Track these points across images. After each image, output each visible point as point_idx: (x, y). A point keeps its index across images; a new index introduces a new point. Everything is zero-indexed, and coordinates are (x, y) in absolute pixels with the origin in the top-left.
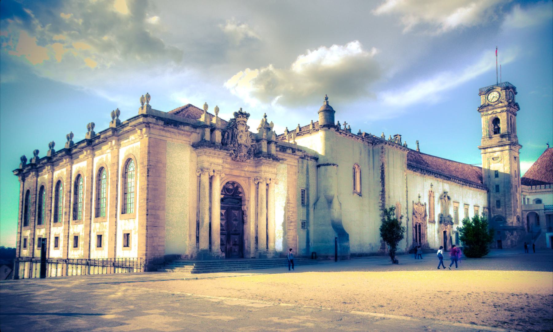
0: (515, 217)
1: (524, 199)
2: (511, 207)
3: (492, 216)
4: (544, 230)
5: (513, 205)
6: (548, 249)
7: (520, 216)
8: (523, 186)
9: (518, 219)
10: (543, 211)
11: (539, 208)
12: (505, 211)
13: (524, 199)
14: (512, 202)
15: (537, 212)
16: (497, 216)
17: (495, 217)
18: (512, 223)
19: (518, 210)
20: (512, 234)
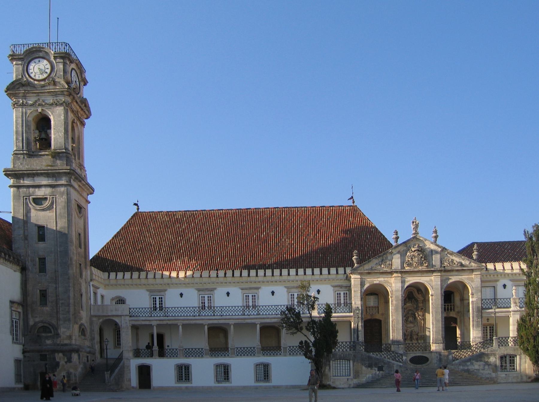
0: (76, 327)
1: (95, 294)
2: (69, 305)
3: (31, 323)
4: (128, 354)
5: (71, 301)
6: (133, 387)
7: (87, 325)
8: (95, 271)
9: (83, 331)
10: (128, 318)
11: (119, 313)
12: (57, 313)
13: (95, 294)
14: (72, 295)
15: (117, 320)
16: (42, 322)
17: (36, 324)
18: (70, 337)
19: (84, 314)
20: (69, 360)
